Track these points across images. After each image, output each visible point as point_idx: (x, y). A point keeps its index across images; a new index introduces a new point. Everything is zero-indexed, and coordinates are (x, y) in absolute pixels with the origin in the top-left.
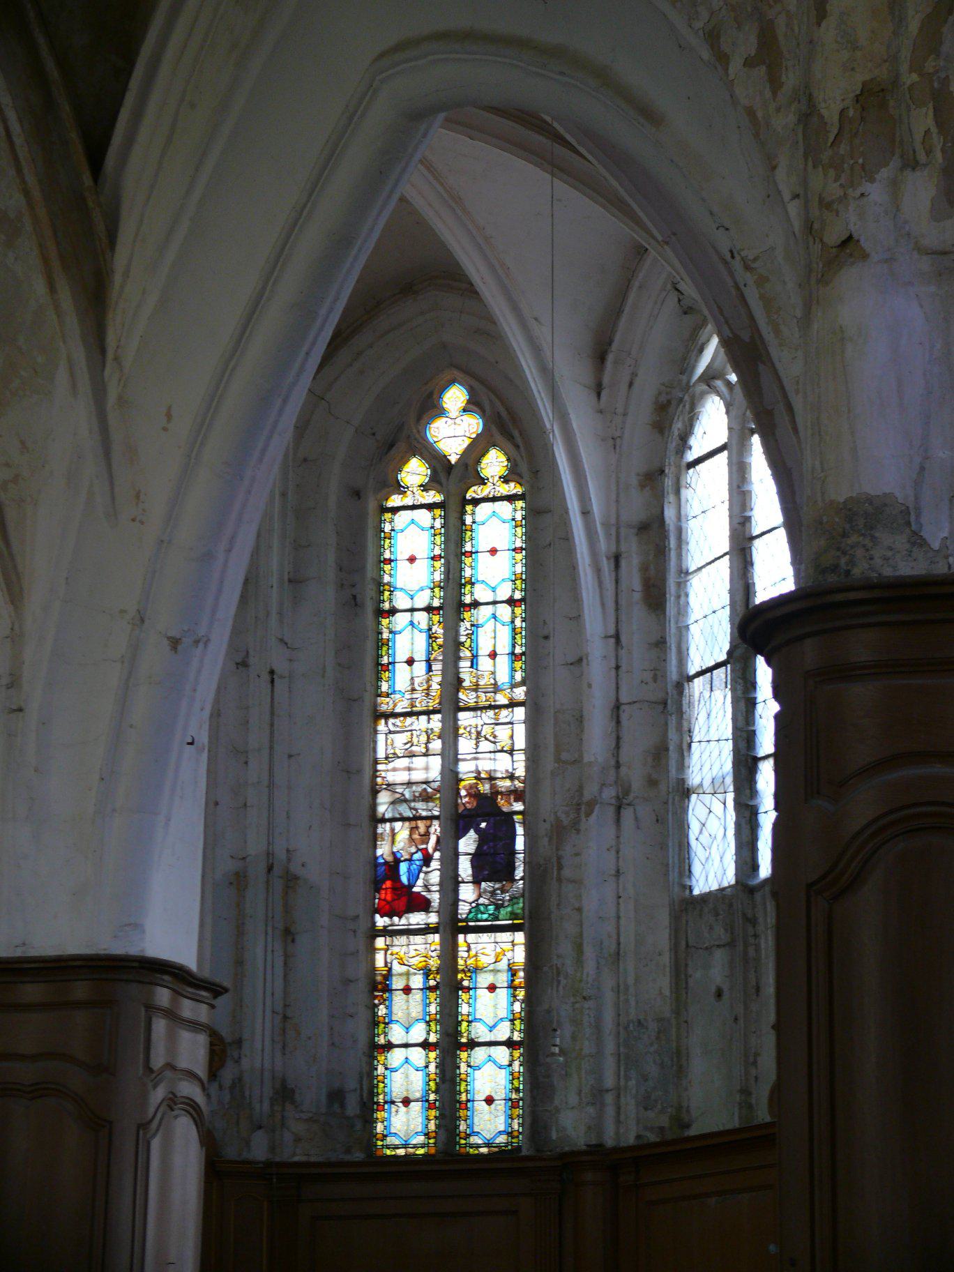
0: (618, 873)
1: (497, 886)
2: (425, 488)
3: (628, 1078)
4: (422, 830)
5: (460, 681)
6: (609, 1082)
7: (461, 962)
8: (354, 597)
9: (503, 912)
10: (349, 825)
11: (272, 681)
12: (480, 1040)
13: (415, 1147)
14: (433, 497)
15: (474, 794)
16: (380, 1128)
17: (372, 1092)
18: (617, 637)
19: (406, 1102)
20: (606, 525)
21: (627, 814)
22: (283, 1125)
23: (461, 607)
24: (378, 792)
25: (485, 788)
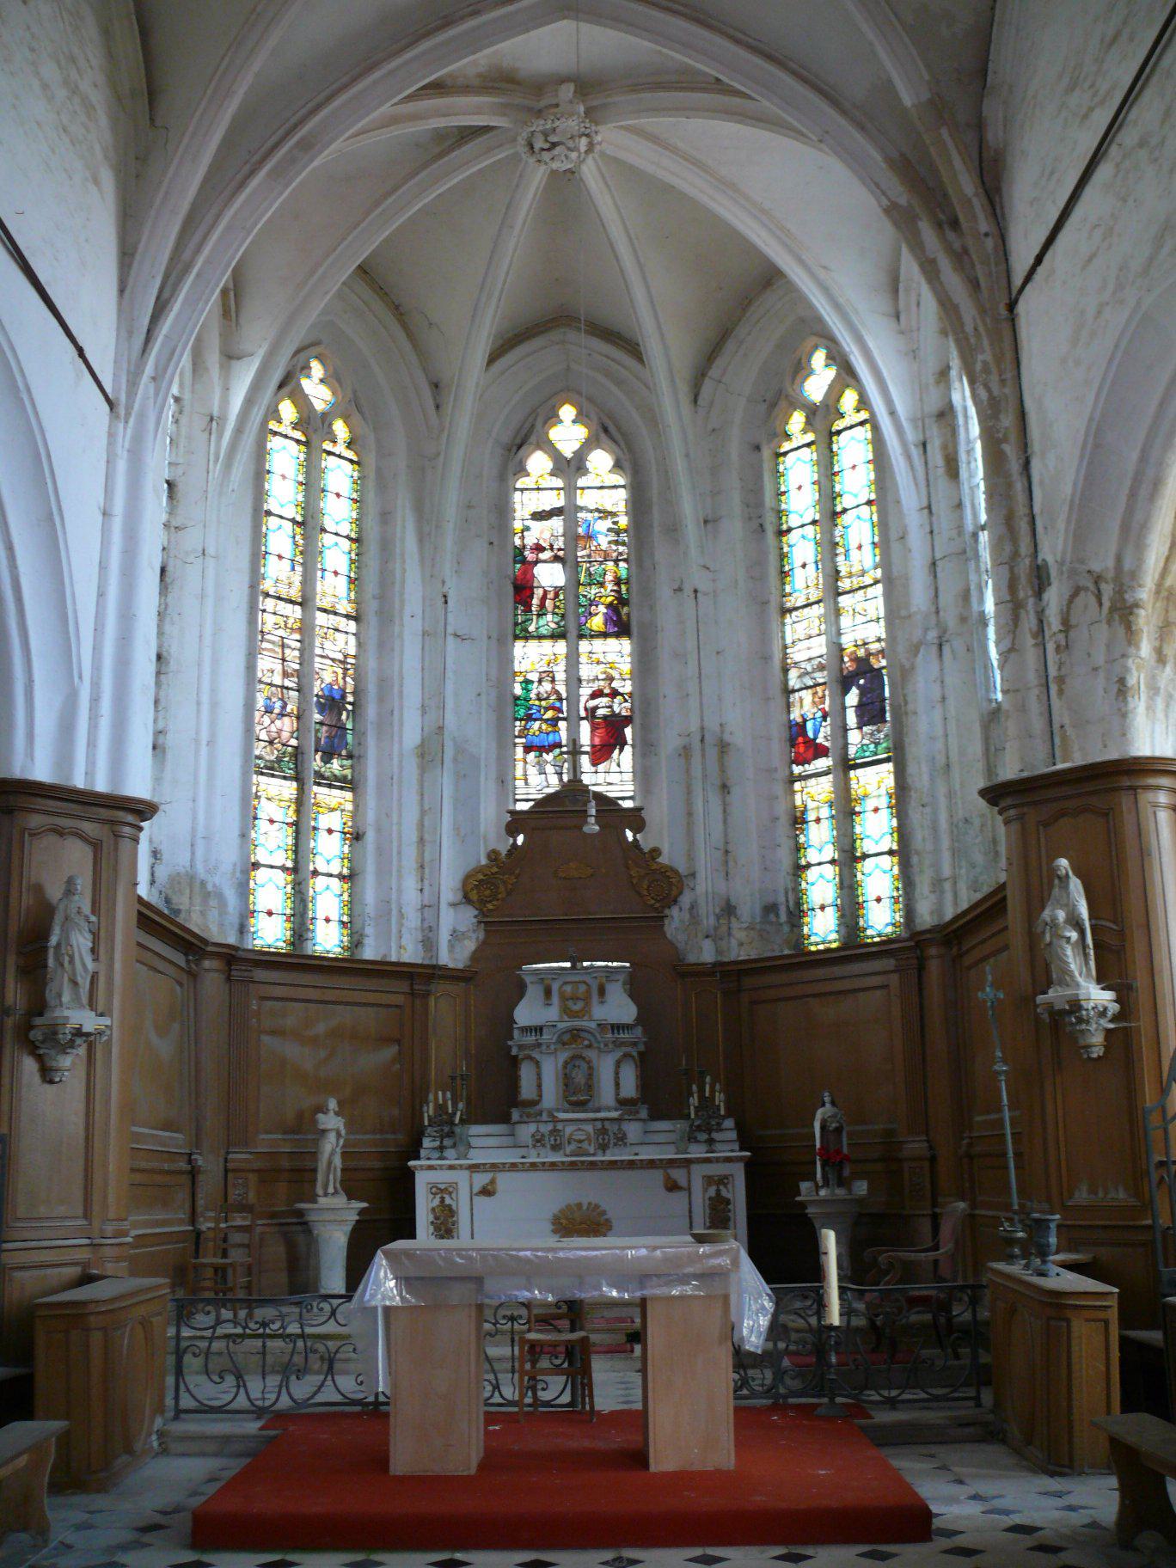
0: (944, 699)
1: (875, 728)
2: (804, 431)
3: (960, 868)
4: (820, 694)
5: (838, 572)
6: (947, 870)
7: (853, 792)
8: (761, 525)
9: (880, 748)
10: (768, 699)
11: (696, 598)
12: (870, 853)
13: (830, 942)
14: (810, 437)
15: (856, 659)
16: (806, 930)
17: (798, 904)
18: (929, 507)
19: (823, 908)
20: (913, 420)
21: (946, 649)
22: (730, 934)
23: (835, 515)
24: (788, 670)
25: (861, 653)
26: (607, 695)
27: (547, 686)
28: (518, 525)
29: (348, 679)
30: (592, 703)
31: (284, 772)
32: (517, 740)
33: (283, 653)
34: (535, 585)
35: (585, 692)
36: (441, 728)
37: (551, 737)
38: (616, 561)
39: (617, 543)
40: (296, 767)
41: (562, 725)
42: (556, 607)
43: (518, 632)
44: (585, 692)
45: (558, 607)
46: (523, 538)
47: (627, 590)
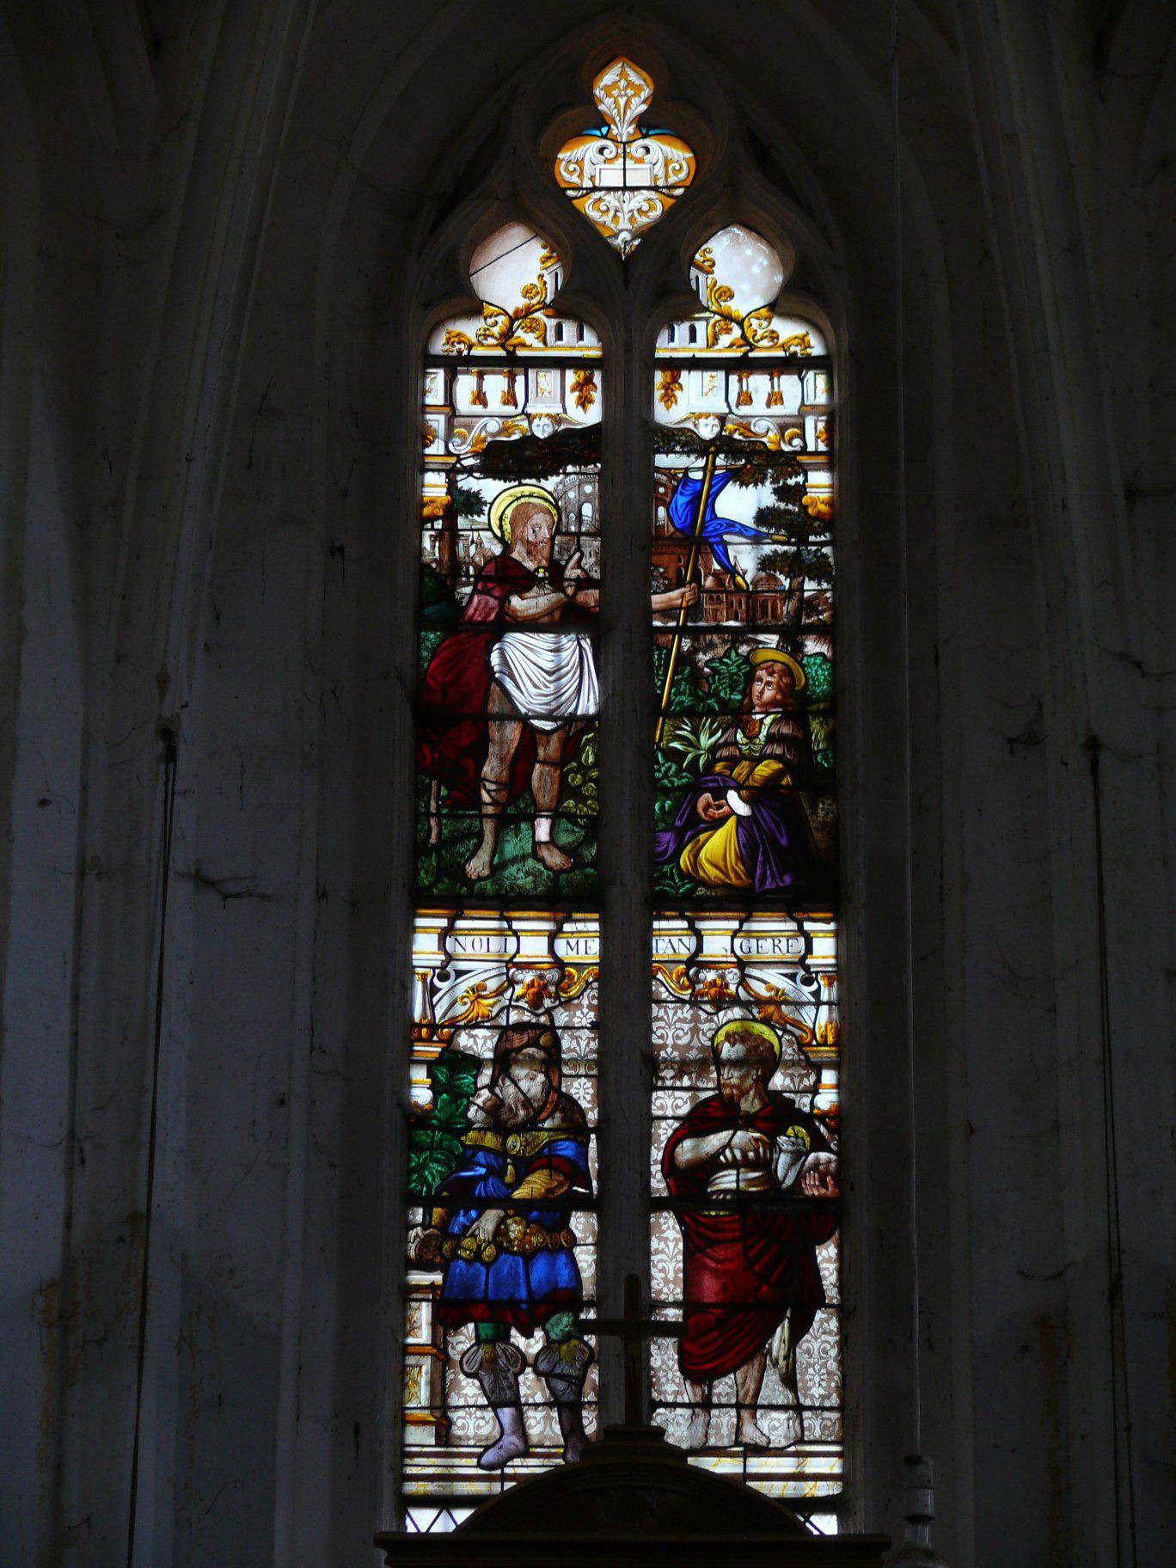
11: (1094, 769)
26: (748, 1122)
27: (530, 1082)
28: (434, 486)
30: (687, 1150)
32: (418, 1278)
34: (494, 707)
35: (671, 1104)
36: (139, 1221)
37: (540, 1269)
38: (792, 638)
39: (794, 565)
41: (581, 1224)
42: (565, 791)
43: (425, 879)
44: (671, 1104)
45: (577, 794)
46: (450, 536)
47: (831, 737)
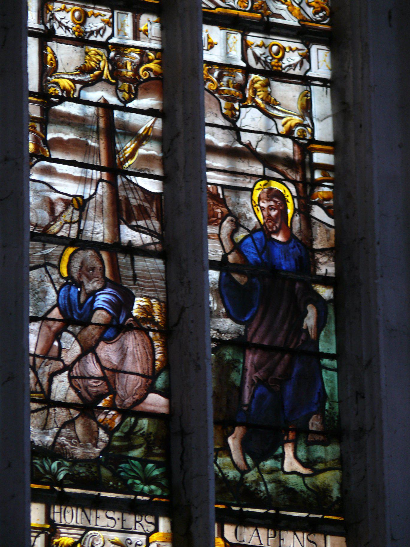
29: (318, 213)
31: (129, 489)
33: (112, 151)
40: (168, 474)
